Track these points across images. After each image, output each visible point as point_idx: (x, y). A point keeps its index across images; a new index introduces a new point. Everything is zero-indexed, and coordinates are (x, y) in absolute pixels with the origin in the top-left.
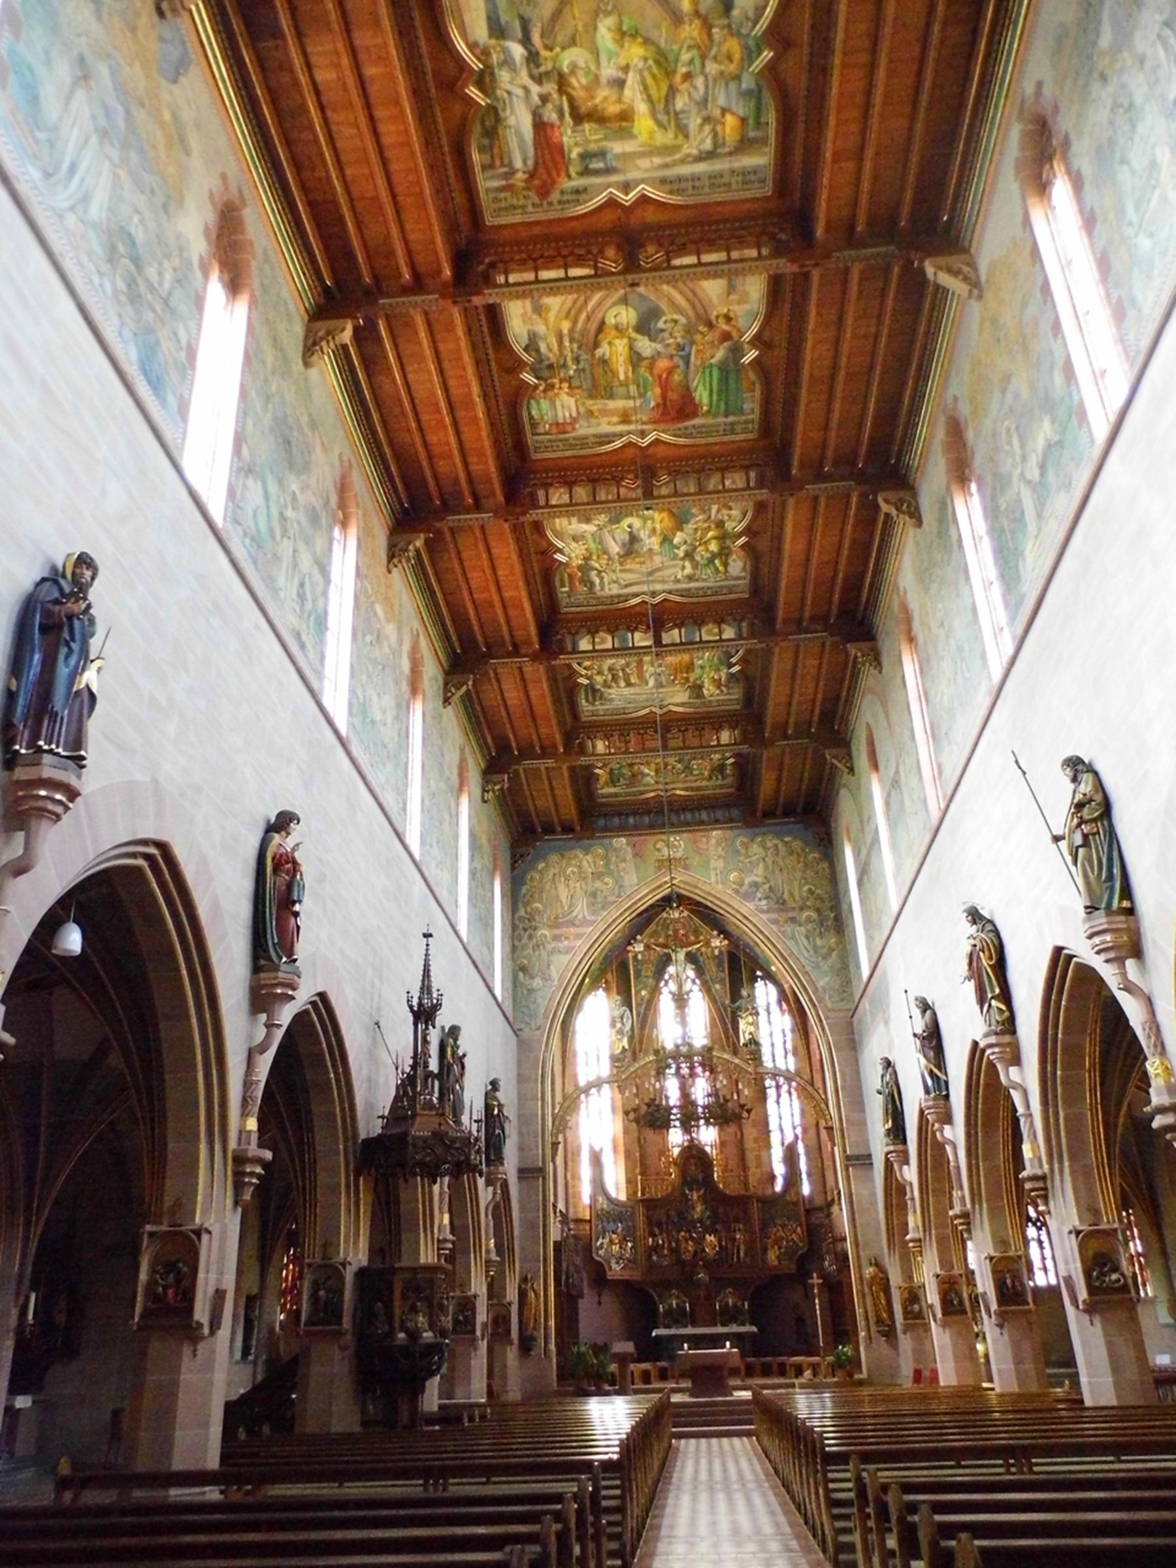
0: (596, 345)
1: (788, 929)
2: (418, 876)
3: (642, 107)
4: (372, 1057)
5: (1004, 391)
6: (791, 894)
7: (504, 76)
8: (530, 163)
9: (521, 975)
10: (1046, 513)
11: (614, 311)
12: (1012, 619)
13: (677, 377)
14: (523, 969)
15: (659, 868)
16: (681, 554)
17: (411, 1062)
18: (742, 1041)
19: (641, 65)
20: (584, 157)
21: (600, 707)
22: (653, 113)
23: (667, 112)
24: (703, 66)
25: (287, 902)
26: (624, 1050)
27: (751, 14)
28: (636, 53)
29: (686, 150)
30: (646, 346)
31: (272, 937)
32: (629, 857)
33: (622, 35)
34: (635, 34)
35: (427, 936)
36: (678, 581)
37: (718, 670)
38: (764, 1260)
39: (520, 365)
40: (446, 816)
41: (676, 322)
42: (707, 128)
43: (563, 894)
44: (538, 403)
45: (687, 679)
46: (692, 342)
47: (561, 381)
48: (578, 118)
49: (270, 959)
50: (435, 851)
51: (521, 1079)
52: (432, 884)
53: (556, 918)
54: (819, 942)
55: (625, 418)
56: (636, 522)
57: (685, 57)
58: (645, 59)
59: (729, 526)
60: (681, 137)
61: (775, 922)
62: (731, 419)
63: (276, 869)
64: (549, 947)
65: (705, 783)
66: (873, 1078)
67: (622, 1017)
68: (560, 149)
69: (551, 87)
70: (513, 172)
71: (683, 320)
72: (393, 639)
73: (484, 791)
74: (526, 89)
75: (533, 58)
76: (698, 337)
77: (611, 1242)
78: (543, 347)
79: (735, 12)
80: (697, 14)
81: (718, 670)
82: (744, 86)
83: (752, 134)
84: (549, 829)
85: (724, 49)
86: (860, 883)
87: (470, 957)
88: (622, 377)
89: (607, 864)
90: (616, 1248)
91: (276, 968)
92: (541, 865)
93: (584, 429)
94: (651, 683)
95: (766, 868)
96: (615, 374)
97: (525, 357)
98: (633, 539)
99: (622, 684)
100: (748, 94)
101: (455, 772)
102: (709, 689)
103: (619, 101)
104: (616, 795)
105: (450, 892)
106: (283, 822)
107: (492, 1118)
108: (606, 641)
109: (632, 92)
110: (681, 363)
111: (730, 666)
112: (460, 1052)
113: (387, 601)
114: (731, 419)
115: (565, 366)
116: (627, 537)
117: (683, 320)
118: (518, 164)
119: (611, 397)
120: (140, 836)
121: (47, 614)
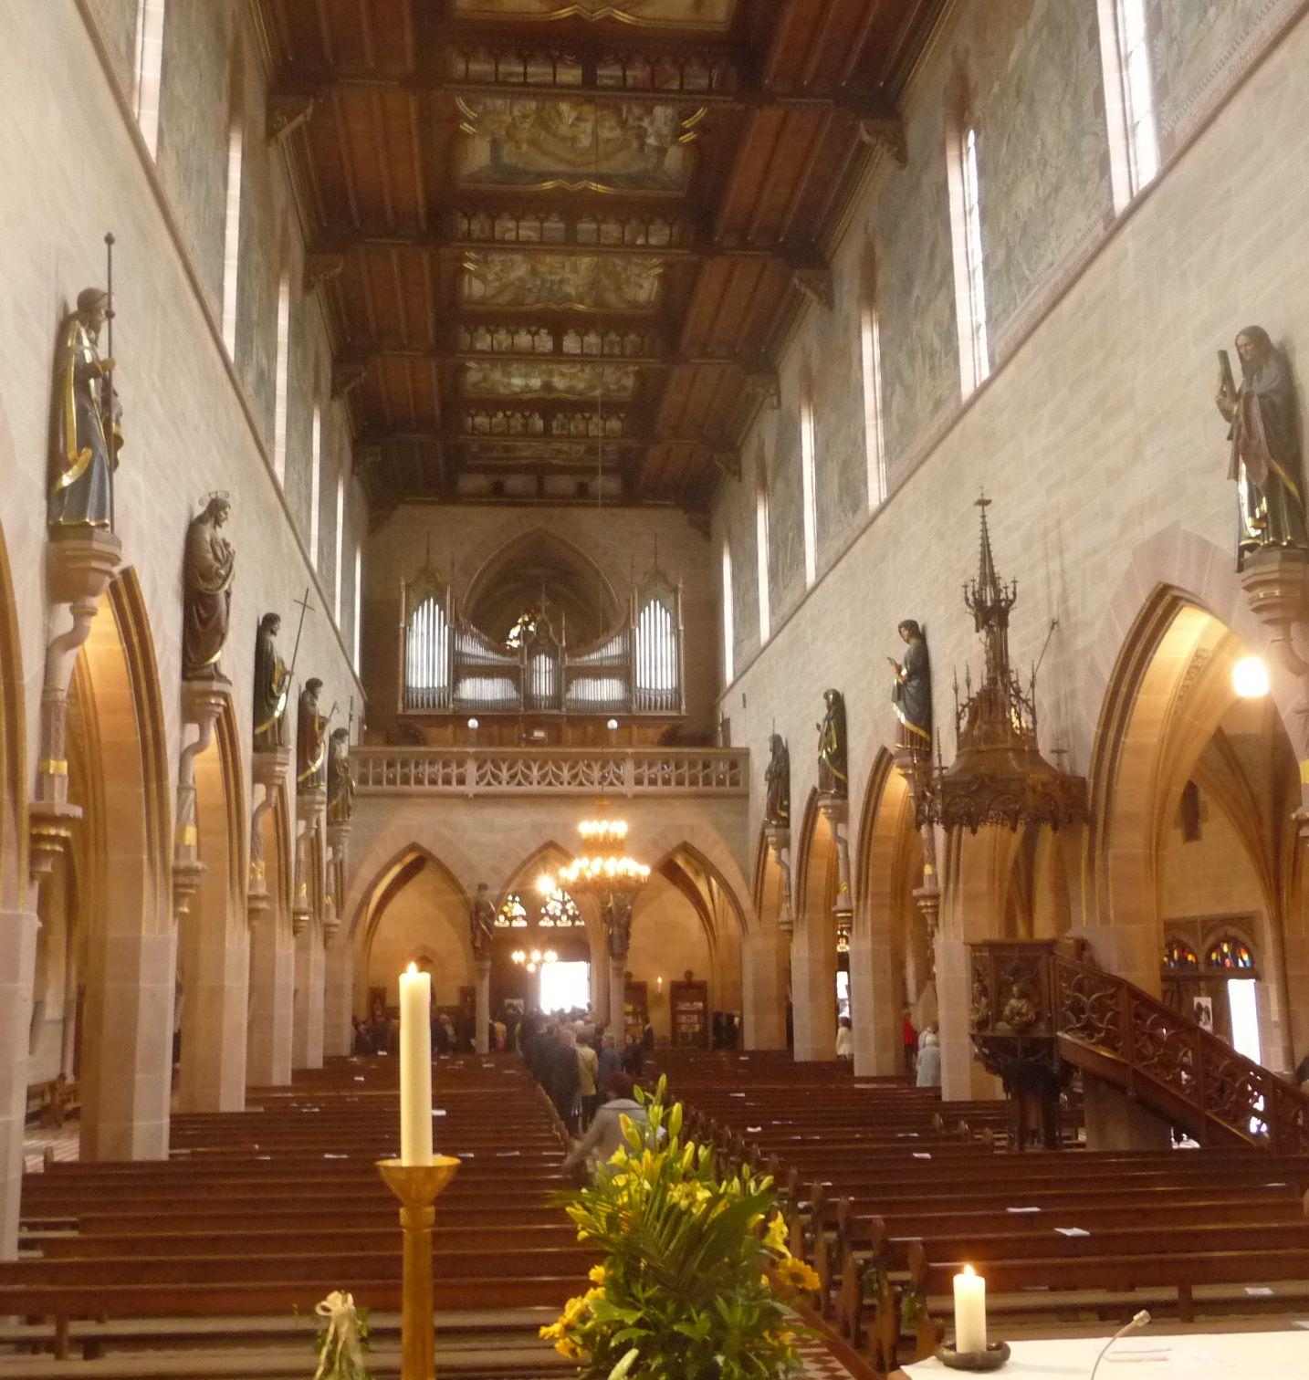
7: (665, 131)
24: (513, 119)
33: (574, 139)
34: (563, 139)
57: (526, 126)
69: (631, 122)
74: (652, 123)
80: (516, 142)
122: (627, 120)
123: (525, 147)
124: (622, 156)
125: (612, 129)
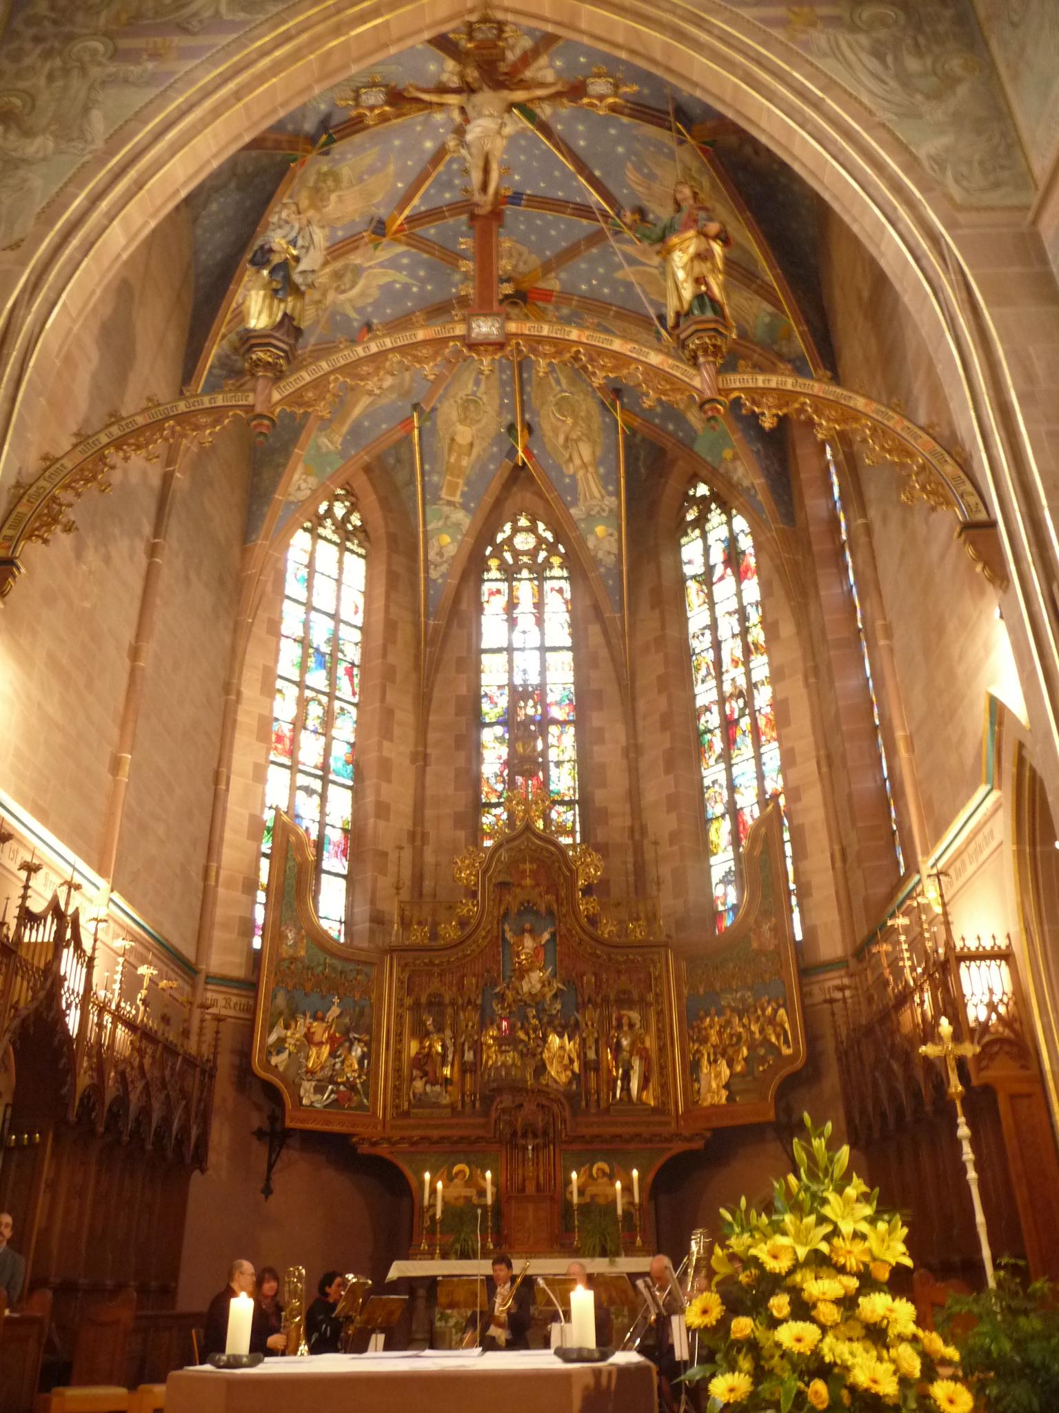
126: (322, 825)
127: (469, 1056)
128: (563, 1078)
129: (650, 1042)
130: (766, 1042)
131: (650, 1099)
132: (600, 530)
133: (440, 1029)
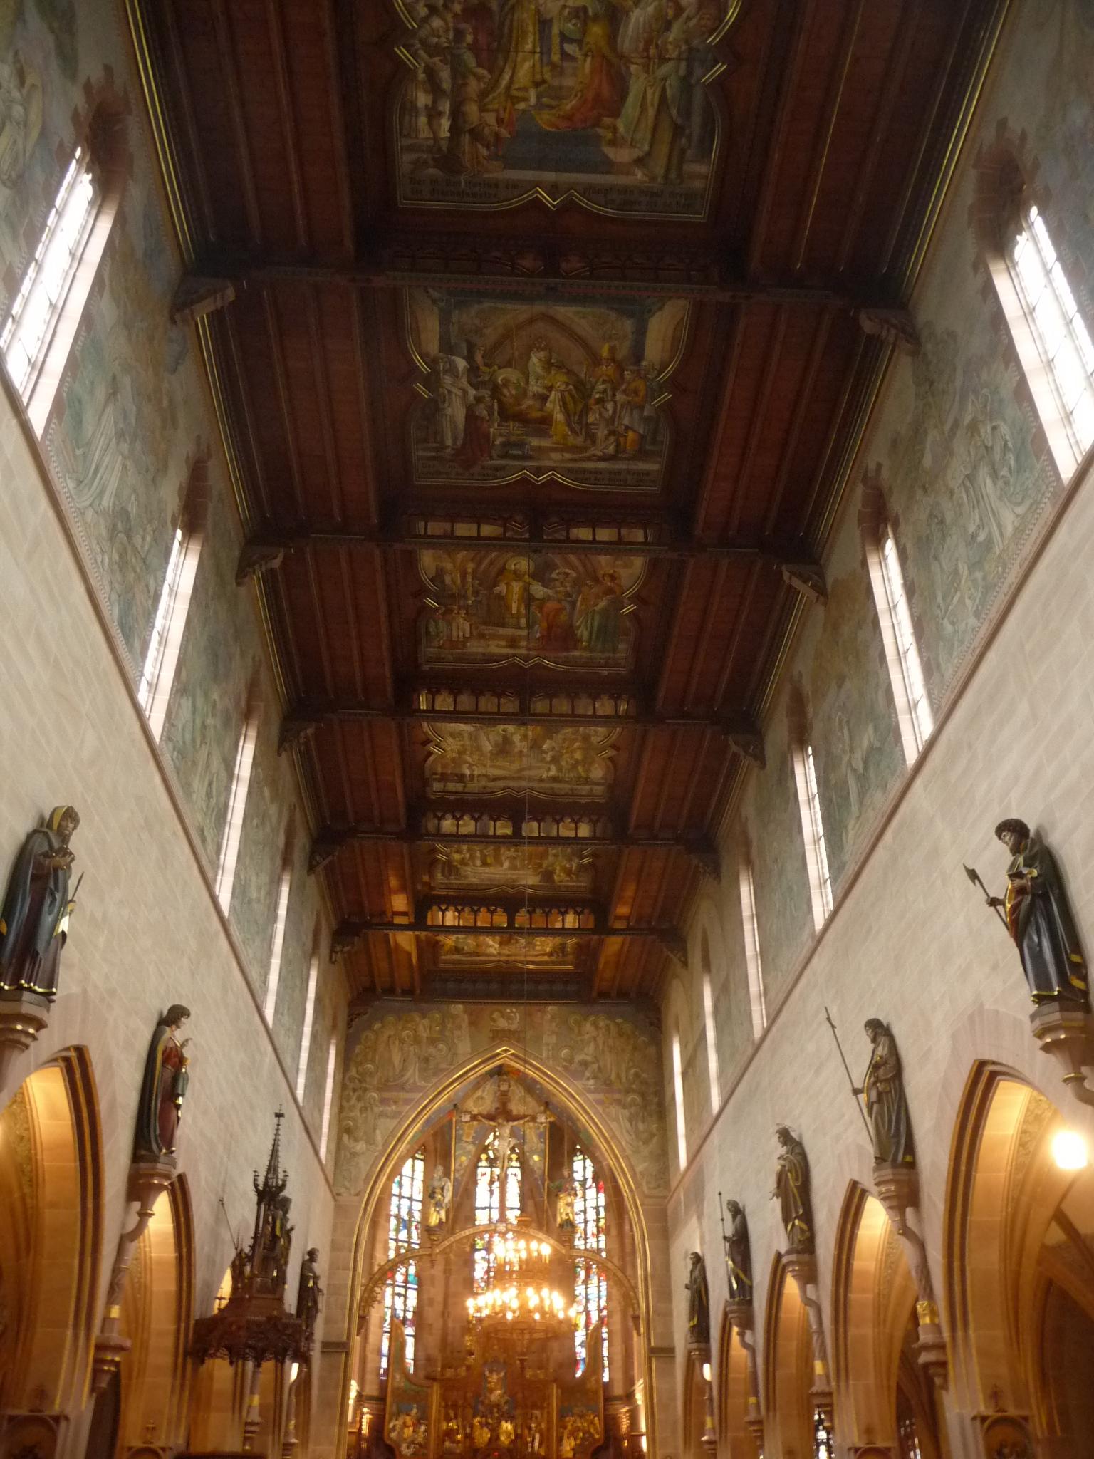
0: (496, 584)
1: (613, 1110)
2: (269, 1048)
3: (559, 417)
4: (215, 1238)
5: (840, 687)
6: (618, 1076)
8: (459, 443)
9: (345, 1137)
10: (867, 801)
11: (516, 560)
12: (834, 879)
13: (563, 617)
14: (348, 1131)
15: (493, 1039)
16: (548, 758)
17: (251, 1242)
18: (559, 1220)
19: (563, 388)
20: (507, 444)
21: (453, 880)
22: (568, 423)
23: (580, 423)
24: (614, 395)
25: (172, 1093)
26: (441, 1222)
27: (657, 367)
28: (560, 381)
29: (592, 451)
30: (538, 590)
31: (155, 1129)
32: (465, 1025)
33: (548, 365)
34: (560, 366)
35: (279, 1115)
36: (541, 780)
37: (570, 860)
38: (558, 1451)
39: (422, 592)
40: (298, 983)
41: (567, 575)
42: (612, 439)
43: (397, 1059)
44: (436, 622)
45: (540, 865)
46: (579, 592)
47: (460, 608)
48: (505, 416)
49: (150, 1150)
50: (286, 1020)
51: (335, 1246)
52: (280, 1051)
53: (387, 1081)
54: (641, 1127)
55: (513, 642)
56: (511, 728)
57: (601, 387)
58: (567, 384)
59: (594, 740)
60: (589, 442)
61: (600, 1102)
62: (607, 655)
63: (166, 1060)
64: (376, 1110)
65: (546, 958)
66: (681, 1273)
67: (442, 1189)
68: (487, 436)
69: (486, 393)
70: (443, 447)
71: (574, 574)
72: (274, 820)
73: (332, 951)
74: (465, 392)
75: (473, 370)
76: (585, 589)
77: (405, 1425)
78: (448, 580)
79: (644, 363)
80: (613, 360)
81: (570, 860)
82: (645, 414)
83: (648, 447)
84: (390, 991)
85: (633, 385)
86: (684, 1074)
87: (304, 1122)
88: (514, 611)
89: (442, 1032)
90: (409, 1431)
91: (155, 1159)
92: (377, 1026)
93: (475, 647)
94: (506, 865)
95: (597, 1046)
96: (509, 608)
97: (431, 585)
98: (507, 740)
99: (478, 863)
100: (647, 420)
101: (310, 936)
102: (559, 877)
103: (541, 410)
104: (459, 962)
105: (293, 1058)
106: (174, 1016)
107: (308, 1295)
108: (468, 826)
109: (553, 405)
110: (568, 606)
111: (582, 857)
112: (289, 1226)
113: (273, 783)
114: (607, 655)
115: (465, 597)
116: (500, 739)
117: (574, 574)
118: (449, 442)
119: (503, 625)
120: (68, 1044)
121: (38, 865)
122: (493, 397)
123: (605, 352)
124: (491, 334)
125: (506, 383)
126: (405, 1311)
127: (468, 1430)
128: (507, 1442)
129: (543, 1426)
130: (589, 1432)
131: (542, 1453)
132: (536, 1158)
133: (456, 1417)
